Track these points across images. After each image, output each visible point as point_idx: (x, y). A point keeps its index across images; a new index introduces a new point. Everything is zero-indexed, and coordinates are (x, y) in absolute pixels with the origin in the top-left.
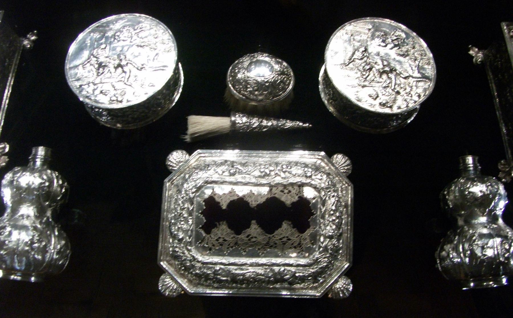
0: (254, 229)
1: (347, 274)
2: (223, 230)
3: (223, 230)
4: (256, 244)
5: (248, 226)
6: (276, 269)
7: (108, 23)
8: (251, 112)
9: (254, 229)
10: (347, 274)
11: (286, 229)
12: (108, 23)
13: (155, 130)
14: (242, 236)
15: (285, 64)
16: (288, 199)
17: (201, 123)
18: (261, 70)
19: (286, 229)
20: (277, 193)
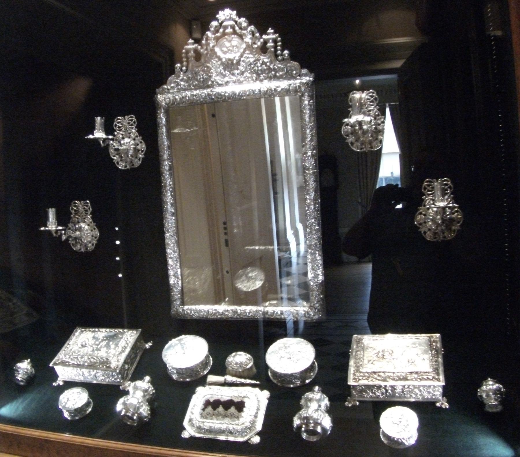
0: (221, 409)
1: (259, 434)
2: (210, 409)
4: (221, 415)
5: (218, 407)
6: (227, 425)
7: (182, 339)
8: (233, 375)
9: (221, 409)
10: (259, 434)
11: (233, 410)
12: (182, 339)
13: (194, 379)
14: (216, 411)
15: (249, 356)
16: (236, 400)
17: (211, 378)
18: (240, 359)
19: (233, 410)
20: (232, 398)
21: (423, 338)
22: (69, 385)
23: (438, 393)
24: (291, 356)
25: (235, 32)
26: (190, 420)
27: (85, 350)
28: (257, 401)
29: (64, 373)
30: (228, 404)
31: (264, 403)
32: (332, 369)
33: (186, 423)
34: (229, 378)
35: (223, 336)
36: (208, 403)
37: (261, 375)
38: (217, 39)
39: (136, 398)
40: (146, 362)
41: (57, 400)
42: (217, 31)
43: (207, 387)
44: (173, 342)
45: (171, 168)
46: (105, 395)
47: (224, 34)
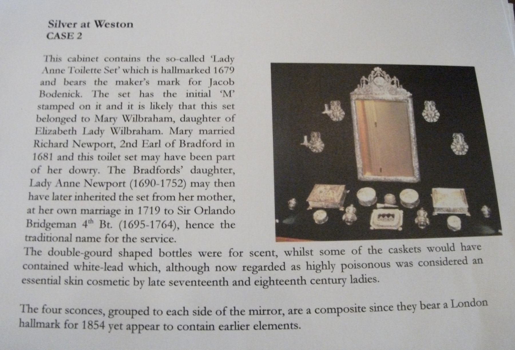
0: (386, 217)
2: (381, 217)
3: (381, 217)
9: (386, 217)
11: (391, 217)
19: (391, 217)
21: (458, 190)
22: (315, 209)
23: (466, 210)
24: (410, 197)
25: (381, 76)
26: (373, 222)
27: (322, 195)
28: (399, 214)
29: (312, 205)
30: (388, 215)
31: (402, 215)
32: (426, 201)
33: (371, 224)
34: (386, 205)
35: (382, 188)
36: (380, 216)
37: (399, 204)
38: (375, 77)
39: (350, 214)
40: (350, 199)
41: (312, 217)
42: (374, 74)
43: (378, 210)
44: (362, 190)
45: (357, 124)
46: (334, 214)
47: (377, 76)
